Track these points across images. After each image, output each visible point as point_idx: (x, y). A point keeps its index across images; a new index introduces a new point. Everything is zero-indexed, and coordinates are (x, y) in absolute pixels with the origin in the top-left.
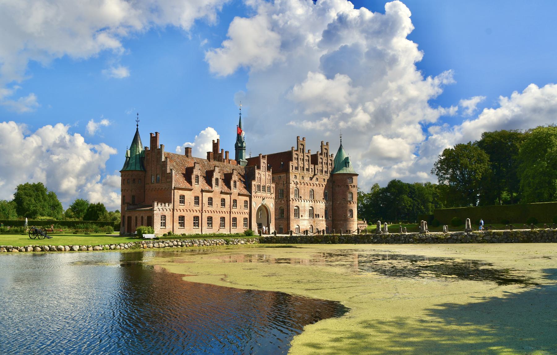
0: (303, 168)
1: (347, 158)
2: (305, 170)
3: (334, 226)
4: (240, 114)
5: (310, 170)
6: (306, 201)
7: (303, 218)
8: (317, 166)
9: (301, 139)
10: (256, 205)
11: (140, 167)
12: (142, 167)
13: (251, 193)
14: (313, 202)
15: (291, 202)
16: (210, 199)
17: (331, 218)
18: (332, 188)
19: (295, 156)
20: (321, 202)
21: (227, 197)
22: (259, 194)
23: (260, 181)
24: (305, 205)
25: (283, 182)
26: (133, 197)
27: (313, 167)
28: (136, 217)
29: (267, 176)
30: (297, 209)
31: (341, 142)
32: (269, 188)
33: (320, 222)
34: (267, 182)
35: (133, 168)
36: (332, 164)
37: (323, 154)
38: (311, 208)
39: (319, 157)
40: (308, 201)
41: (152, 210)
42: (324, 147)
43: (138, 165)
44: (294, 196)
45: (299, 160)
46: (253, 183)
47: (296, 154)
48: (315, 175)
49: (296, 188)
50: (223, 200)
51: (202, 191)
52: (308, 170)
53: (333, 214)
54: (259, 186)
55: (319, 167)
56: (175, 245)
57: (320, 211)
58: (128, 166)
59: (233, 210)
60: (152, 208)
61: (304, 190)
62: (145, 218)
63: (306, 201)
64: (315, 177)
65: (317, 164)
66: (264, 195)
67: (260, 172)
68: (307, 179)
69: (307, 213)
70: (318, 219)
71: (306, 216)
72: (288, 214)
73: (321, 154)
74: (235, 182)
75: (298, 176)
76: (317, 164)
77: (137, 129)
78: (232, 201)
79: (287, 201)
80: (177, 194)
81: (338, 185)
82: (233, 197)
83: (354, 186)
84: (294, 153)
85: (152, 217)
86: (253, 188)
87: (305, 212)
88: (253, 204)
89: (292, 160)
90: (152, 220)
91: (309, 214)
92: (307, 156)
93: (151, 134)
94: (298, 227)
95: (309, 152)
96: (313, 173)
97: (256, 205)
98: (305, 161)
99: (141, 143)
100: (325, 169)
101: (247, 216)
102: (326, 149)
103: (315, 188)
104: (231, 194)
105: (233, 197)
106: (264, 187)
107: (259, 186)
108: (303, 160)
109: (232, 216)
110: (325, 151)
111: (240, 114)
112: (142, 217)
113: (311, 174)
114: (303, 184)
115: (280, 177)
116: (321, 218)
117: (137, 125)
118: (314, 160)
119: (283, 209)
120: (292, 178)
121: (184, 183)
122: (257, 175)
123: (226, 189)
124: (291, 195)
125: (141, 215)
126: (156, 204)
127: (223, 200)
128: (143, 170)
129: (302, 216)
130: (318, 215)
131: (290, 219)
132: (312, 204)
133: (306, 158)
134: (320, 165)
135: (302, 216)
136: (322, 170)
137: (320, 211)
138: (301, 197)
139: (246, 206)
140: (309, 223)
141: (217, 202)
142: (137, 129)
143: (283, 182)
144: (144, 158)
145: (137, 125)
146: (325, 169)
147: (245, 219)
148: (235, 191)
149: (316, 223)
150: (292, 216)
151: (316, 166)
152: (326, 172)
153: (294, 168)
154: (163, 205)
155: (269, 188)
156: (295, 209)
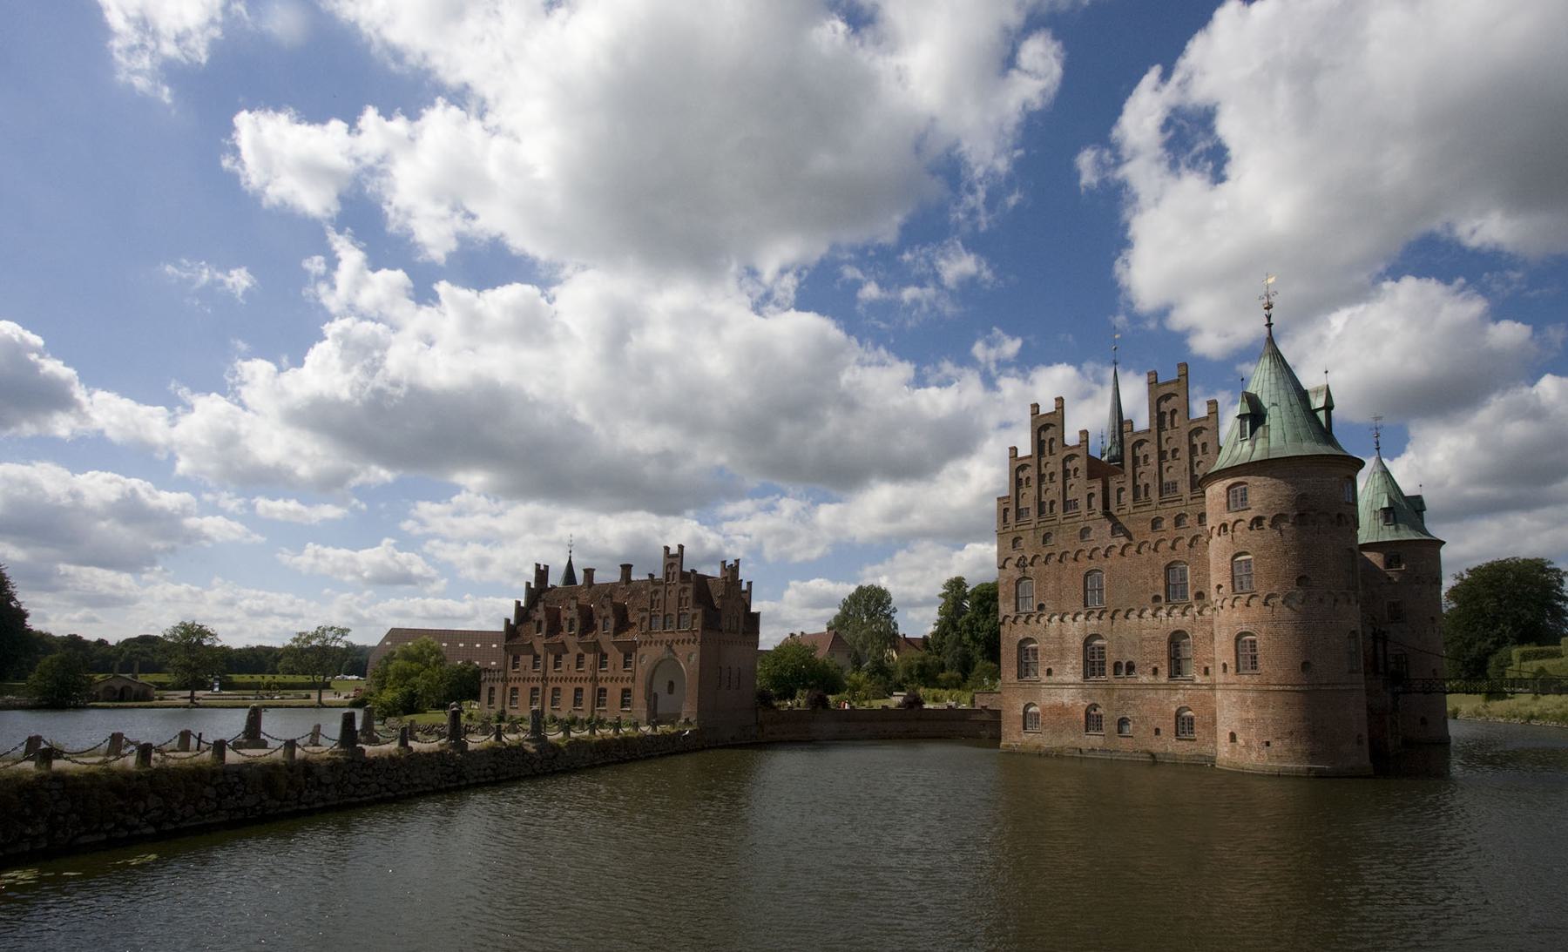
7: (1055, 678)
33: (1140, 692)
44: (1013, 607)
49: (1025, 578)
57: (1141, 648)
61: (1059, 579)
63: (1068, 618)
70: (1133, 681)
71: (1071, 671)
132: (1099, 626)
135: (1049, 672)
137: (1141, 648)
140: (1083, 697)
149: (1120, 698)
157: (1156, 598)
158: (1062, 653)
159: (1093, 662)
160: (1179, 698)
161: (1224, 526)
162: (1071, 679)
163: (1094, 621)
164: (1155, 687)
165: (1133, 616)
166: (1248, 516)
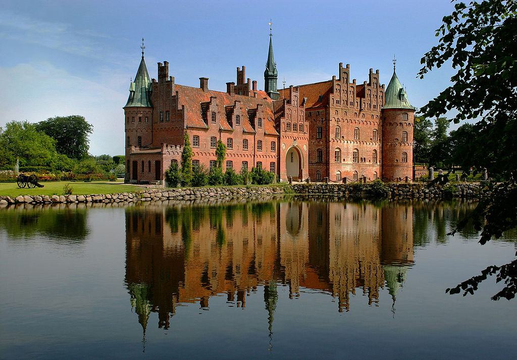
0: (347, 101)
1: (401, 90)
2: (349, 104)
3: (384, 173)
4: (271, 35)
5: (356, 104)
6: (349, 142)
7: (346, 162)
8: (364, 99)
9: (344, 66)
10: (285, 148)
11: (147, 102)
12: (148, 103)
13: (279, 133)
14: (358, 142)
15: (331, 143)
16: (230, 140)
17: (380, 162)
18: (382, 126)
19: (336, 87)
20: (368, 143)
21: (250, 138)
22: (289, 133)
23: (291, 118)
24: (348, 146)
25: (322, 119)
26: (140, 138)
27: (359, 101)
28: (143, 162)
29: (299, 112)
30: (338, 152)
31: (394, 69)
32: (301, 126)
34: (299, 119)
35: (139, 105)
36: (382, 97)
37: (372, 84)
38: (356, 151)
39: (367, 88)
40: (352, 142)
41: (161, 154)
42: (373, 76)
43: (145, 100)
45: (342, 92)
46: (282, 120)
47: (338, 84)
48: (361, 110)
50: (245, 141)
51: (220, 131)
52: (352, 104)
53: (382, 158)
54: (289, 125)
55: (366, 100)
56: (187, 195)
58: (132, 102)
59: (258, 153)
60: (159, 150)
62: (153, 163)
63: (349, 142)
64: (362, 113)
65: (364, 97)
66: (295, 135)
67: (291, 107)
68: (350, 116)
69: (351, 157)
71: (350, 160)
72: (327, 157)
73: (369, 85)
74: (260, 119)
75: (340, 111)
76: (364, 97)
77: (143, 57)
78: (256, 142)
79: (326, 141)
80: (191, 134)
81: (390, 123)
82: (258, 138)
83: (409, 124)
84: (335, 83)
85: (161, 162)
86: (283, 126)
87: (348, 155)
88: (283, 146)
89: (332, 92)
90: (161, 165)
91: (354, 158)
92: (352, 87)
93: (159, 64)
94: (339, 173)
95: (354, 82)
96: (359, 107)
97: (285, 148)
98: (349, 93)
99: (147, 74)
100: (374, 103)
101: (275, 160)
102: (375, 78)
103: (360, 126)
104: (255, 134)
105: (258, 138)
106: (295, 125)
107: (289, 125)
108: (347, 91)
109: (257, 160)
110: (374, 81)
111: (271, 35)
112: (150, 162)
113: (356, 108)
114: (346, 121)
115: (319, 112)
116: (367, 163)
117: (143, 53)
118: (361, 92)
119: (322, 152)
120: (332, 112)
121: (200, 122)
122: (287, 111)
123: (249, 128)
124: (330, 135)
125: (148, 159)
126: (165, 145)
127: (245, 141)
128: (150, 106)
129: (344, 159)
130: (365, 159)
131: (329, 163)
133: (350, 89)
134: (367, 99)
135: (344, 159)
136: (370, 105)
138: (343, 137)
139: (273, 148)
141: (238, 142)
142: (143, 57)
143: (322, 119)
144: (152, 91)
145: (143, 53)
146: (374, 103)
147: (272, 164)
148: (259, 131)
150: (332, 160)
151: (363, 99)
152: (374, 106)
153: (335, 102)
154: (174, 148)
155: (301, 126)
156: (336, 152)
157: (371, 139)
158: (348, 154)
159: (356, 156)
160: (374, 169)
161: (401, 123)
162: (350, 162)
163: (355, 144)
164: (370, 165)
165: (365, 144)
166: (407, 122)
